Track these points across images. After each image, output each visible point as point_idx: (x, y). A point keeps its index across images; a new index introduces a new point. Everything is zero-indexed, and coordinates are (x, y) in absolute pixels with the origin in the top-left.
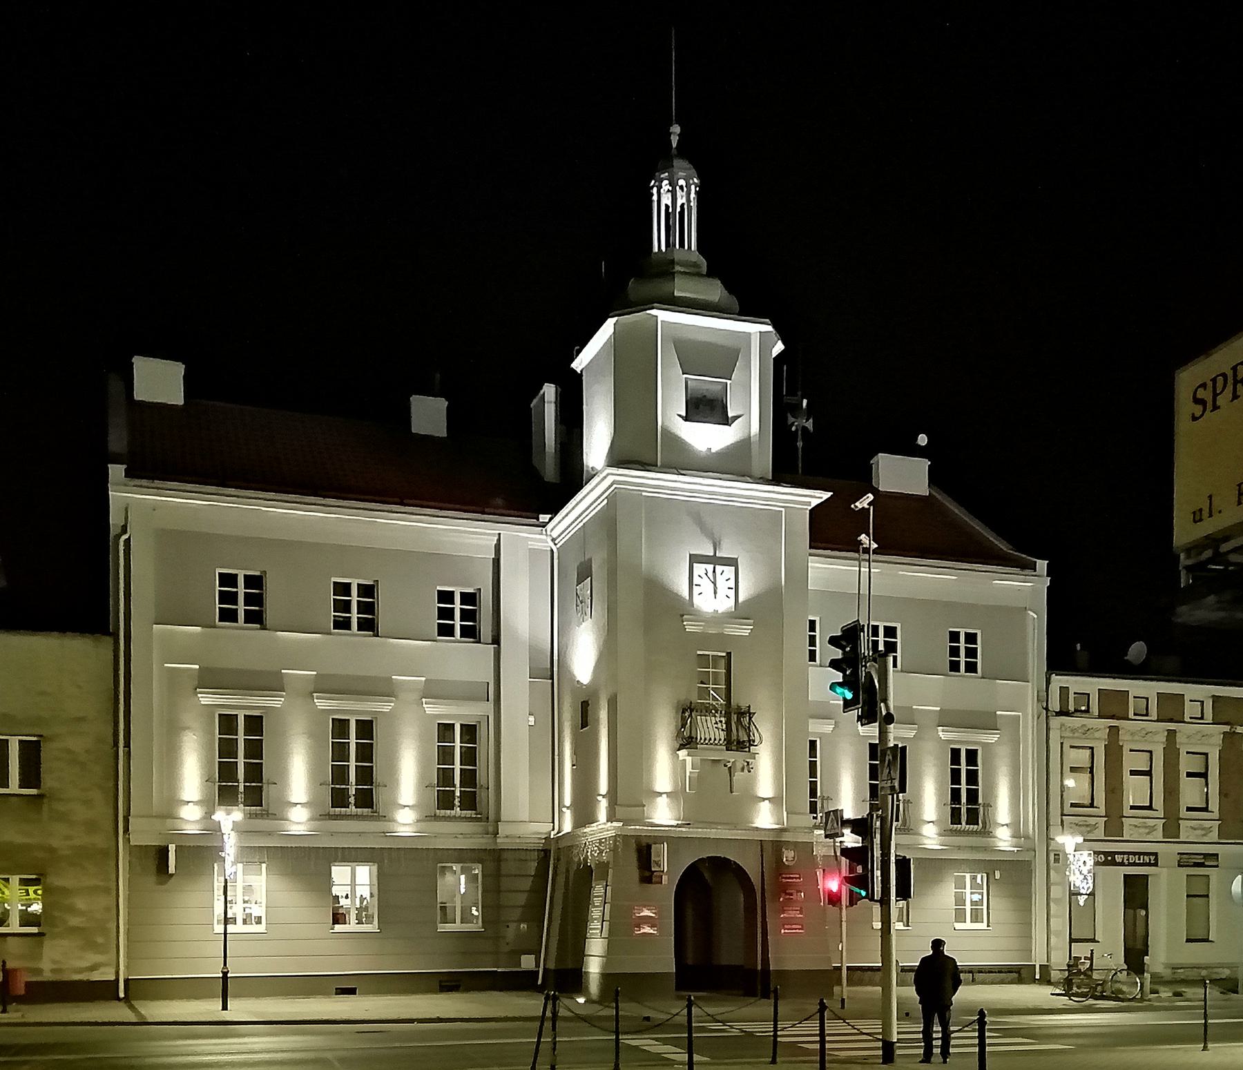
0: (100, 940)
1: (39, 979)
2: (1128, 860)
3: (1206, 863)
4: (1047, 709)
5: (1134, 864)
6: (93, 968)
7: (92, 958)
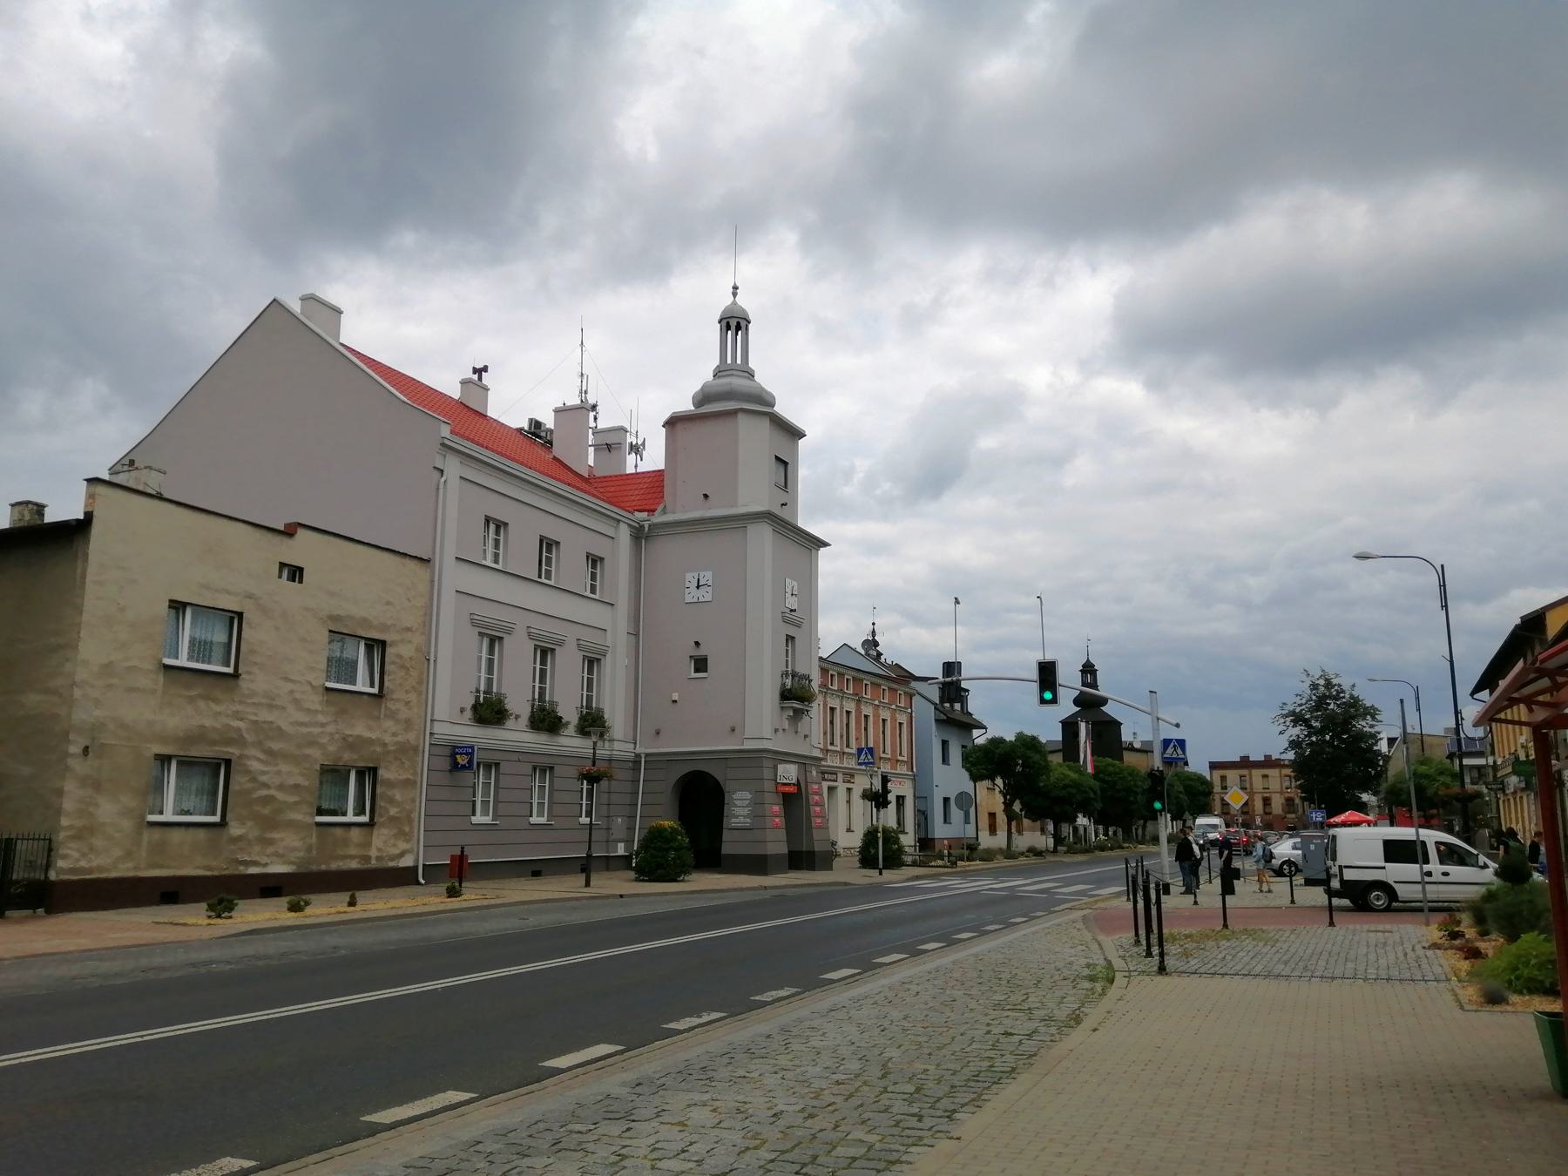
0: (407, 829)
6: (402, 855)
7: (403, 846)
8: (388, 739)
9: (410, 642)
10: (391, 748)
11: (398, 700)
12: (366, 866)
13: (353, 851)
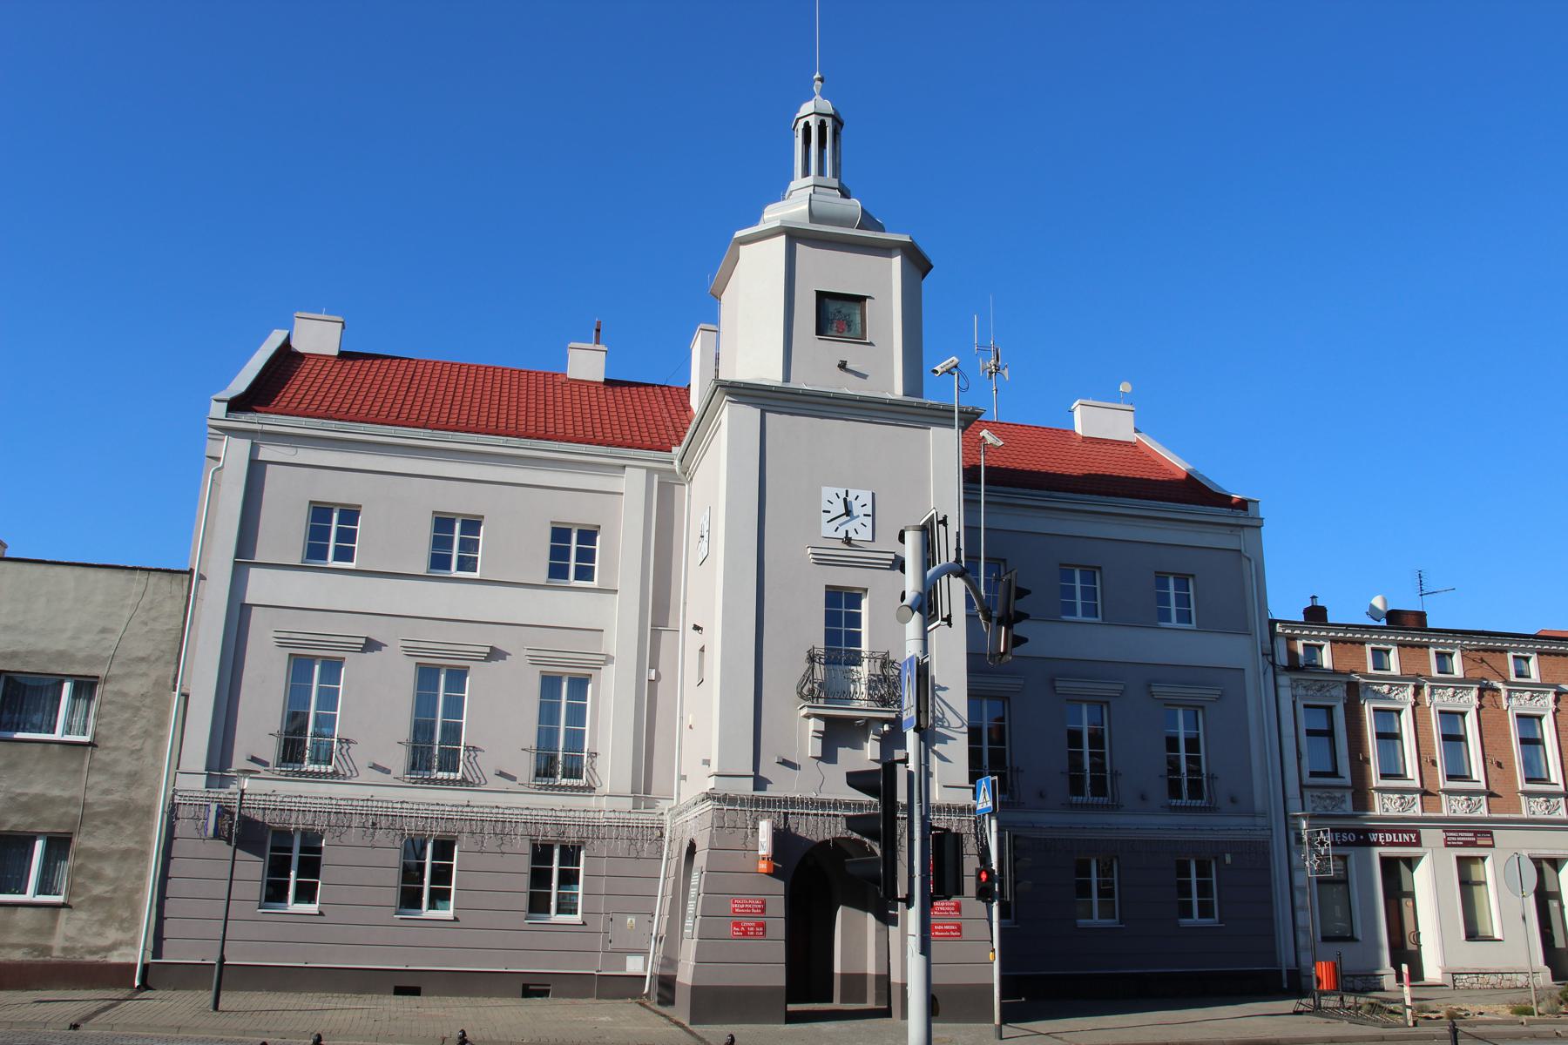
0: (126, 914)
1: (48, 958)
2: (1385, 839)
3: (1479, 842)
4: (1273, 664)
5: (1392, 844)
7: (112, 935)
8: (91, 797)
9: (145, 675)
10: (97, 809)
11: (116, 749)
12: (41, 959)
13: (14, 938)
